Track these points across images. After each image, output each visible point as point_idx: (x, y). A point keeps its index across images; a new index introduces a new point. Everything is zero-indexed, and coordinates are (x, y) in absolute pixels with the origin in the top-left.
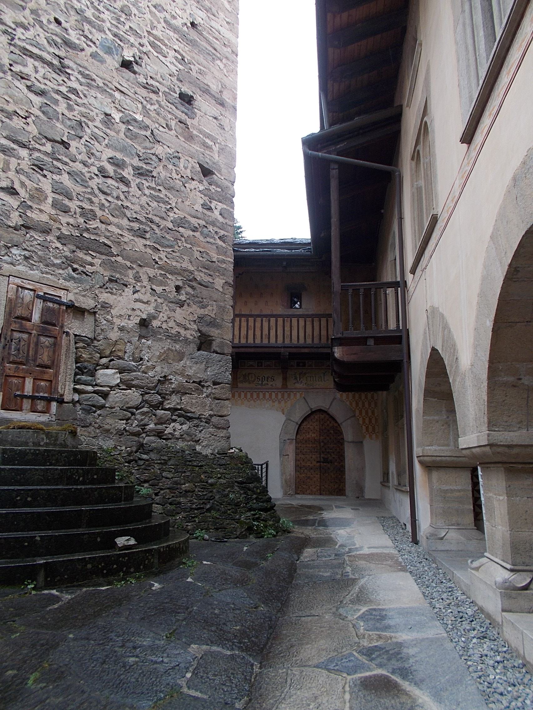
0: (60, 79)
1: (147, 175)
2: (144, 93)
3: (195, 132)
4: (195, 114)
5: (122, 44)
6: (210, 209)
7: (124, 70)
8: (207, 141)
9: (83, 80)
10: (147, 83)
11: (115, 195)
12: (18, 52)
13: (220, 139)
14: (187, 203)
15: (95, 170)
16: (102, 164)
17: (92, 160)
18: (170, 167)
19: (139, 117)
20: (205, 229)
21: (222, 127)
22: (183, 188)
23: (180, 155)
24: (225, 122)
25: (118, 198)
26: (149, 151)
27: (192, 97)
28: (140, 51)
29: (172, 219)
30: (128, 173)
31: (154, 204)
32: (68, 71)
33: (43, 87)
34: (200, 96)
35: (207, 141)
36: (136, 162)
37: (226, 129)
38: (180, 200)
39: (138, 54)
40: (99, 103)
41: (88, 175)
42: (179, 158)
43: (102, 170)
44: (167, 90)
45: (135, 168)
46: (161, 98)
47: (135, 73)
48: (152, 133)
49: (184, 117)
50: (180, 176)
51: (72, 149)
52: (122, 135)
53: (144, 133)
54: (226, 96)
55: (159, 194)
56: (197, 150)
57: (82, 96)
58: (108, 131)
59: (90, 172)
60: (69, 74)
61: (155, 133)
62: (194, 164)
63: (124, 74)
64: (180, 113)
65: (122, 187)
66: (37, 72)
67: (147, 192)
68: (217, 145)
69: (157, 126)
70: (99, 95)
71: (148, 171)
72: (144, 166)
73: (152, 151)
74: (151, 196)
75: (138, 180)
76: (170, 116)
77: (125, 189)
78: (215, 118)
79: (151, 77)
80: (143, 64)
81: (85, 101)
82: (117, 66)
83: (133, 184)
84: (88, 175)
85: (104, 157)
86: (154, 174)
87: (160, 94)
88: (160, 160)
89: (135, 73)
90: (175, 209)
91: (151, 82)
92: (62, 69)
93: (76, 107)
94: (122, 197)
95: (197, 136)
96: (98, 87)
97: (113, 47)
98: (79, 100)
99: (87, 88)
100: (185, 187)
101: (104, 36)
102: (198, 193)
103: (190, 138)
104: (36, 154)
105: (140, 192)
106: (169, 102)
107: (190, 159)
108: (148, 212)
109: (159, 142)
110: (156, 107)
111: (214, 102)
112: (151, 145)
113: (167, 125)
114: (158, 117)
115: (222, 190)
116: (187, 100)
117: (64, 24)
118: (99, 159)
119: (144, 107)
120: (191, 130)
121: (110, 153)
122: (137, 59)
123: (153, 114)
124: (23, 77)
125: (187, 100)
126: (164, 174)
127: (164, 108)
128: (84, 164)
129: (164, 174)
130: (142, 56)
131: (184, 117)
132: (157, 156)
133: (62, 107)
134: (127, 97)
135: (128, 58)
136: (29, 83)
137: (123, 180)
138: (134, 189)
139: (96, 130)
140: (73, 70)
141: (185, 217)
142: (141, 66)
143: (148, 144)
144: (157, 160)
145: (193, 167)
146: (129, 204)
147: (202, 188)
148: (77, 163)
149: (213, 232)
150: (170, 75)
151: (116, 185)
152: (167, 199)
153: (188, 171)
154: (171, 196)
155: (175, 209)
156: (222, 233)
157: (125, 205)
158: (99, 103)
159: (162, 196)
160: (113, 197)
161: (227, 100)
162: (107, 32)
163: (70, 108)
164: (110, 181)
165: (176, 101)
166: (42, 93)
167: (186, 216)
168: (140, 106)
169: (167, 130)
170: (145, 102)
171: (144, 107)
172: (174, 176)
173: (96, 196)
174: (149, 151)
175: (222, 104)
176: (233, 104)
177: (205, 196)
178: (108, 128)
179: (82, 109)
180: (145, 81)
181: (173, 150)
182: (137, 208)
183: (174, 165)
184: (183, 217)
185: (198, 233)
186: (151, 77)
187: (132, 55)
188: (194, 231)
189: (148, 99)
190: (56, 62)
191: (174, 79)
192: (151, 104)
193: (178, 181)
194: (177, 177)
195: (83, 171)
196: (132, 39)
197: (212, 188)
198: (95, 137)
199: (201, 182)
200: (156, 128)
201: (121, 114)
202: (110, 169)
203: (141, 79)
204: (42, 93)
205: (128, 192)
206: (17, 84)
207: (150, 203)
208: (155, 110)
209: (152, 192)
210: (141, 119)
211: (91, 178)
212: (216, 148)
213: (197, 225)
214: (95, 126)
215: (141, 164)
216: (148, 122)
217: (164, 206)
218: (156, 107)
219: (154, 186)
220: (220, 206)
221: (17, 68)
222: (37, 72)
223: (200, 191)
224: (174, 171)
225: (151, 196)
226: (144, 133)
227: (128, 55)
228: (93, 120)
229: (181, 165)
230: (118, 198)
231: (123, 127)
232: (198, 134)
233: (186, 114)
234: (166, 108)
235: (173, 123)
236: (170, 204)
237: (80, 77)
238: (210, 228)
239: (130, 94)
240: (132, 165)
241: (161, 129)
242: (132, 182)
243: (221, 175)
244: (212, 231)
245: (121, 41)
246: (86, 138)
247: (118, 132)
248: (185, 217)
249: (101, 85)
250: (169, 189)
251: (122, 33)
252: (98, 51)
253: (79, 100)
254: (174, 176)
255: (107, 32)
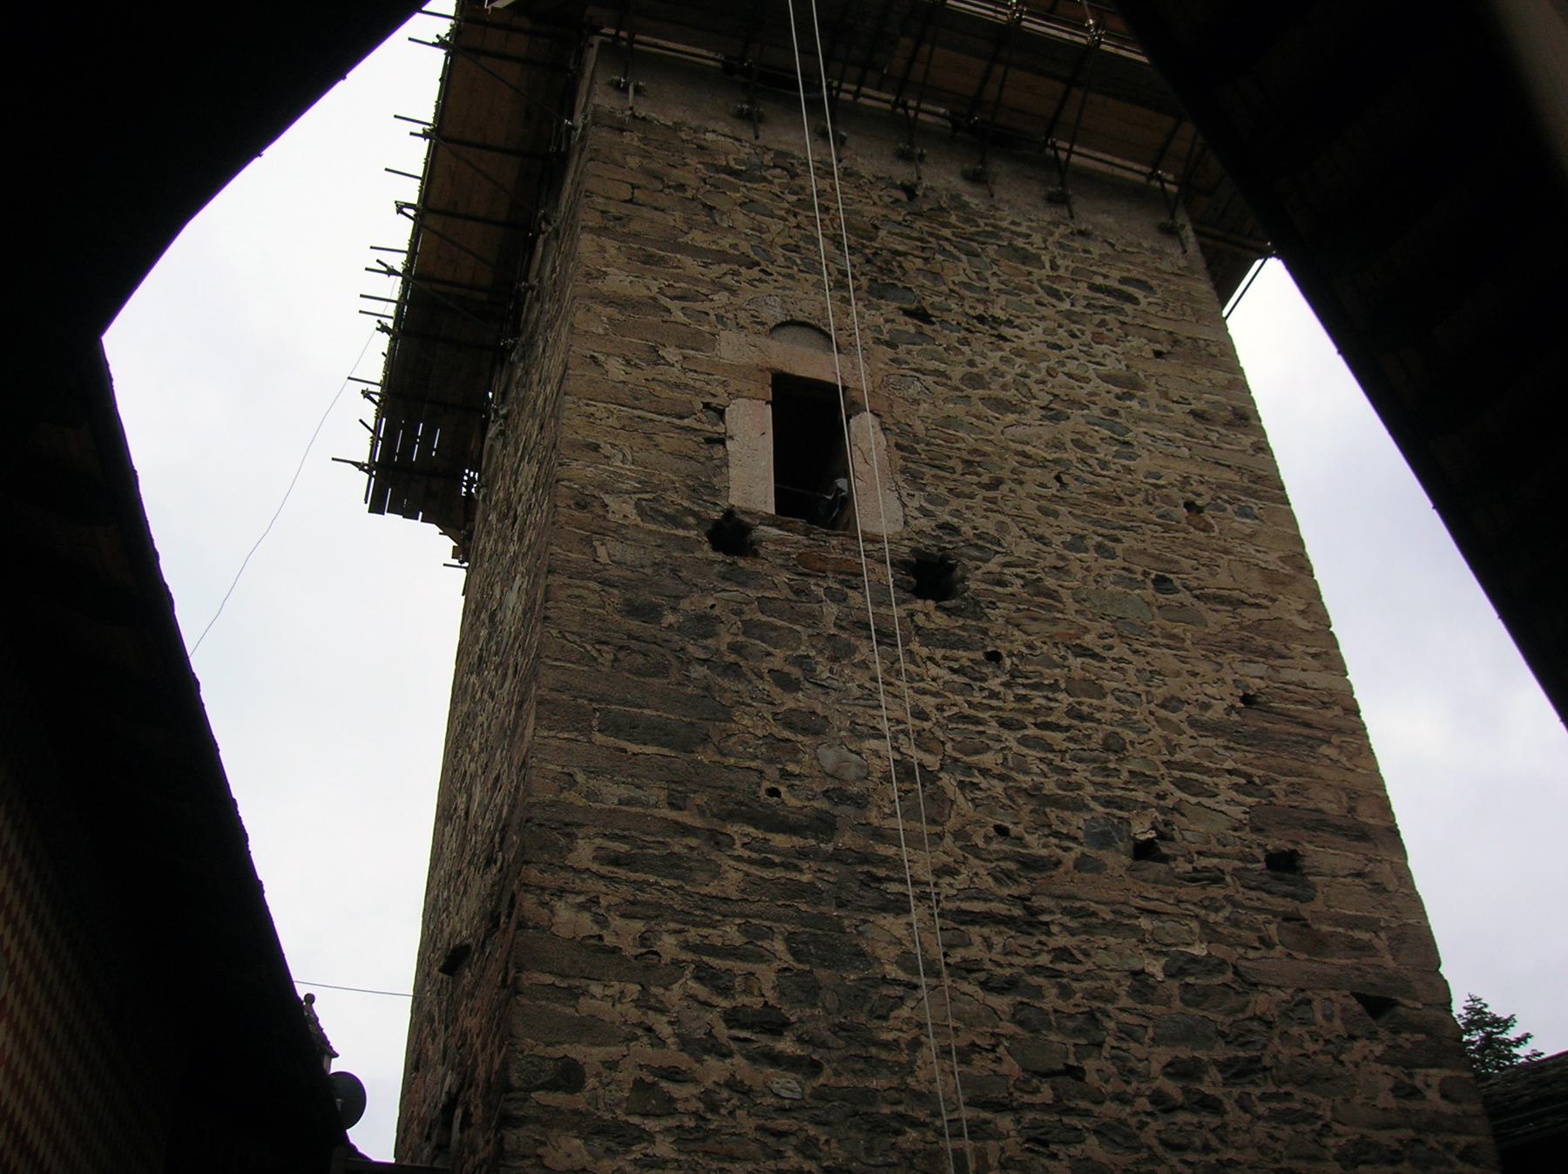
0: (1031, 942)
1: (1253, 1071)
2: (1192, 892)
3: (1325, 928)
4: (1313, 886)
5: (1124, 814)
6: (1414, 1093)
7: (1143, 864)
8: (1358, 934)
9: (1073, 924)
10: (1195, 869)
11: (1198, 1142)
12: (951, 924)
13: (1383, 915)
14: (1358, 1100)
15: (1143, 1103)
16: (1155, 1085)
17: (1134, 1085)
18: (1295, 1030)
19: (1199, 950)
20: (1419, 1148)
21: (1379, 888)
22: (1337, 1069)
23: (1309, 994)
24: (1384, 873)
25: (1207, 1148)
26: (1241, 1016)
27: (1294, 852)
28: (1162, 810)
29: (1335, 1151)
30: (1211, 1084)
31: (1286, 1132)
32: (1045, 918)
33: (1008, 972)
34: (1310, 842)
35: (1358, 934)
36: (1221, 1052)
37: (1391, 888)
38: (1339, 1099)
39: (1160, 818)
40: (1114, 956)
41: (1133, 1121)
42: (1309, 1002)
43: (1158, 1098)
44: (1239, 864)
45: (1223, 1066)
46: (1233, 887)
47: (1165, 859)
48: (1236, 973)
49: (1289, 905)
50: (1321, 1042)
51: (1092, 1078)
52: (1177, 1004)
53: (1218, 980)
54: (1365, 815)
55: (1288, 1104)
56: (1342, 968)
57: (1080, 957)
58: (1149, 1008)
59: (1136, 1113)
60: (1046, 924)
61: (1242, 969)
62: (1346, 1001)
63: (1145, 873)
64: (1280, 901)
65: (1208, 1119)
66: (990, 947)
67: (1261, 1109)
68: (1382, 935)
69: (1241, 951)
70: (1111, 940)
71: (1251, 1060)
72: (1241, 1054)
73: (1249, 1013)
74: (1276, 1116)
75: (1236, 1091)
76: (1261, 918)
77: (1214, 1121)
78: (1359, 875)
79: (1199, 853)
80: (1176, 835)
81: (1089, 965)
82: (1126, 860)
83: (1229, 1105)
84: (1133, 1121)
85: (1156, 1067)
86: (1267, 1061)
87: (1228, 879)
88: (1269, 1025)
89: (1165, 859)
90: (1335, 1126)
91: (1204, 862)
92: (1031, 922)
93: (1075, 985)
94: (1214, 1142)
95: (1332, 934)
96: (1105, 924)
97: (1109, 828)
98: (1078, 969)
99: (1084, 937)
100: (1342, 1063)
101: (1088, 817)
102: (1375, 1067)
103: (1318, 945)
104: (1030, 1116)
105: (1248, 1116)
106: (1251, 888)
107: (1332, 994)
108: (1277, 1155)
109: (1255, 985)
110: (1226, 912)
111: (1344, 840)
112: (1242, 999)
113: (1261, 940)
114: (1237, 932)
115: (1429, 1033)
116: (1284, 863)
117: (1015, 830)
118: (1147, 1077)
119: (1204, 923)
120: (1316, 927)
121: (1163, 1055)
122: (1162, 828)
123: (1225, 930)
124: (967, 969)
125: (1284, 863)
126: (1286, 1053)
127: (1244, 907)
128: (1121, 1099)
129: (1286, 1053)
130: (1169, 817)
131: (1289, 905)
132: (1260, 1019)
133: (1051, 1000)
134: (1165, 918)
135: (1143, 838)
136: (982, 976)
137: (1209, 1105)
138: (1234, 1115)
139: (1125, 1017)
140: (1051, 912)
141: (1363, 1136)
142: (1172, 839)
143: (1233, 1001)
144: (1263, 1028)
145: (1344, 1010)
146: (1231, 1154)
147: (1378, 1049)
148: (1108, 1103)
149: (1441, 1148)
150: (1235, 830)
151: (1195, 1119)
152: (1311, 1110)
153: (1337, 1022)
154: (1317, 1098)
155: (1335, 1126)
156: (1462, 1140)
157: (1225, 1157)
158: (1114, 956)
159: (1297, 1106)
160: (1196, 1150)
161: (1371, 821)
162: (1093, 804)
163: (1066, 992)
164: (1182, 1117)
165: (1265, 879)
166: (1008, 986)
167: (1365, 1131)
168: (1194, 925)
169: (1263, 952)
170: (1203, 912)
171: (1204, 923)
172: (1310, 1047)
173: (1161, 1161)
174: (1241, 1016)
175: (1361, 835)
176: (1386, 824)
177: (1393, 1064)
178: (1147, 1002)
179: (1085, 984)
180: (1189, 867)
181: (1290, 991)
182: (1251, 1155)
183: (1303, 1022)
184: (1356, 1137)
185: (1406, 1164)
186: (1199, 853)
187: (1148, 825)
188: (1393, 1162)
189: (1206, 903)
190: (1017, 912)
191: (1246, 834)
192: (1217, 910)
193: (1321, 1057)
194: (1317, 1047)
195: (1123, 1115)
196: (1140, 795)
197: (1405, 1038)
198: (1127, 1033)
199: (1372, 1036)
200: (1241, 957)
201: (1163, 960)
202: (1172, 1088)
203: (1183, 867)
204: (1008, 986)
205: (1224, 1126)
206: (965, 987)
207: (1277, 1133)
208: (1227, 919)
209: (1274, 1105)
210: (1204, 953)
211: (1142, 1125)
212: (1381, 942)
213: (1396, 1146)
214: (1122, 1008)
215: (1232, 1052)
216: (1220, 951)
217: (1307, 1128)
218: (1226, 912)
219: (1273, 1089)
220: (1436, 1075)
221: (957, 956)
222: (990, 947)
223: (1378, 1060)
224: (1307, 1037)
225: (1276, 1116)
226: (1218, 980)
227: (1142, 830)
228: (1112, 998)
229: (1319, 1017)
230: (1207, 1148)
231: (1174, 986)
232: (1332, 929)
233: (1294, 897)
234: (1247, 903)
235: (1272, 930)
236: (1319, 1118)
237: (1066, 920)
238: (1431, 1140)
239: (1169, 909)
240: (1215, 1062)
241: (1252, 954)
242: (1225, 1101)
243: (1416, 999)
244: (1436, 1146)
245: (1121, 808)
246: (1110, 1041)
247: (1167, 1002)
248: (1363, 1136)
249: (1109, 917)
250: (1309, 1081)
251: (1119, 793)
252: (1086, 850)
253: (1078, 969)
254: (1310, 1047)
255: (1093, 804)
